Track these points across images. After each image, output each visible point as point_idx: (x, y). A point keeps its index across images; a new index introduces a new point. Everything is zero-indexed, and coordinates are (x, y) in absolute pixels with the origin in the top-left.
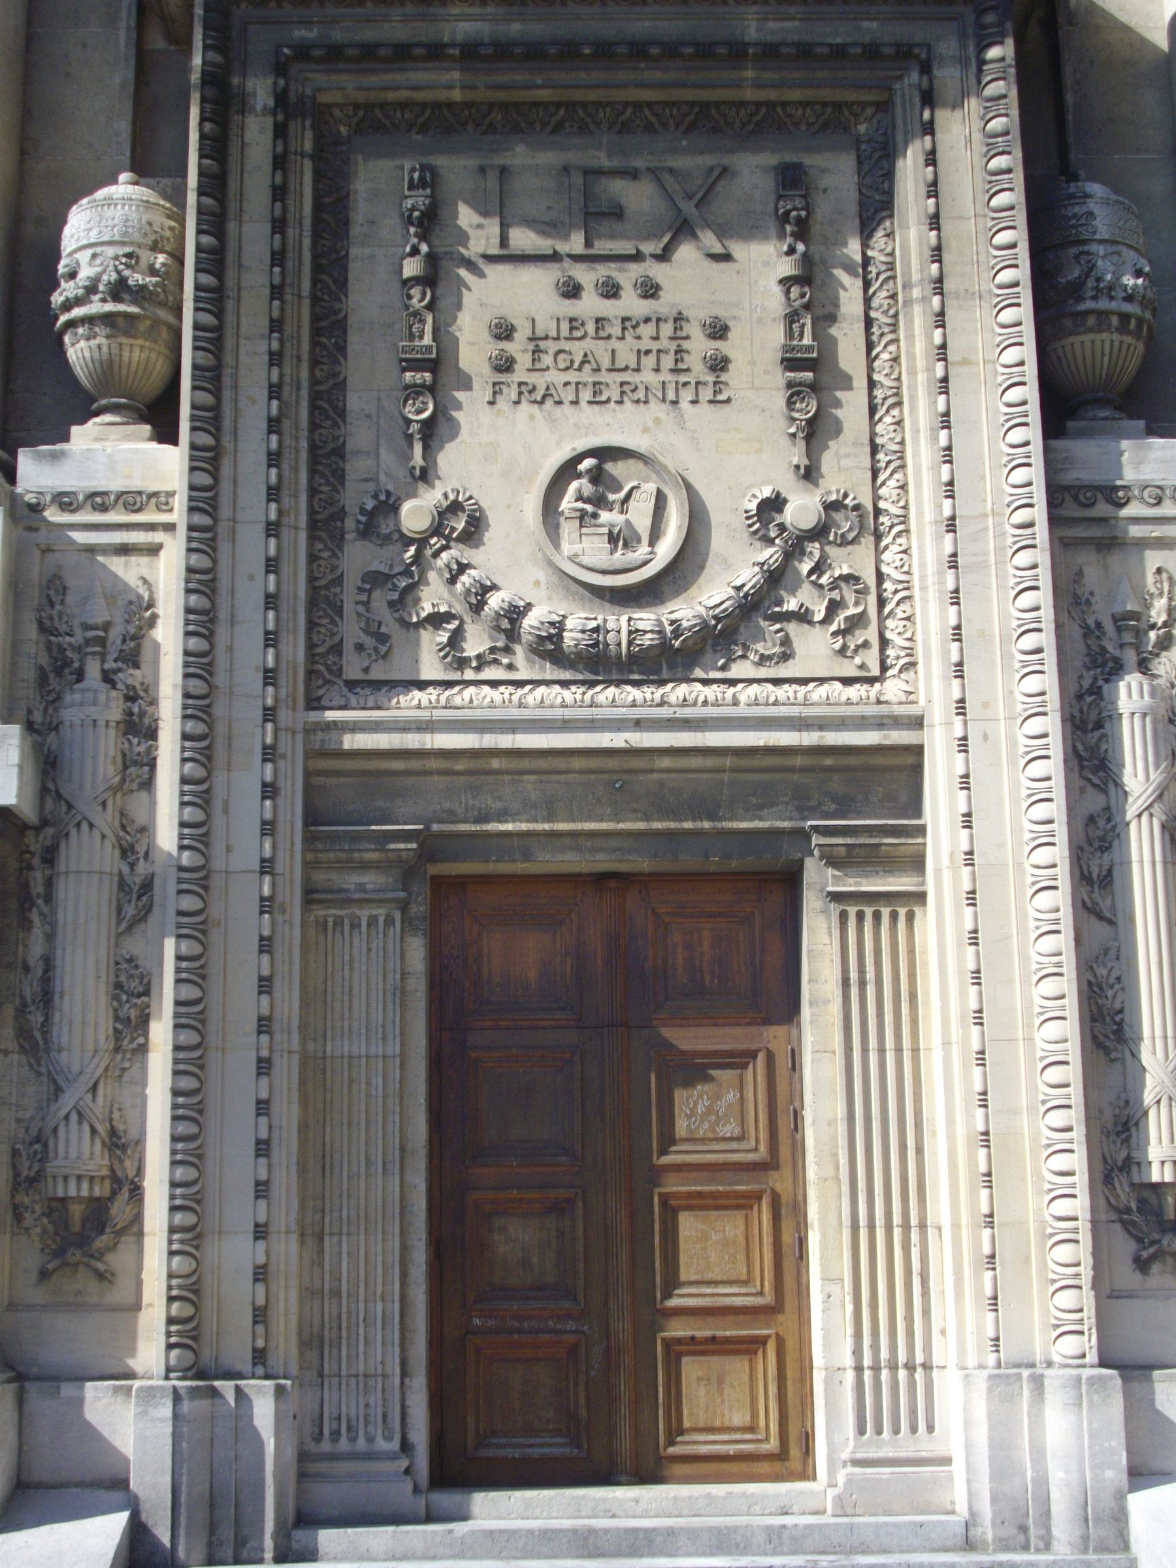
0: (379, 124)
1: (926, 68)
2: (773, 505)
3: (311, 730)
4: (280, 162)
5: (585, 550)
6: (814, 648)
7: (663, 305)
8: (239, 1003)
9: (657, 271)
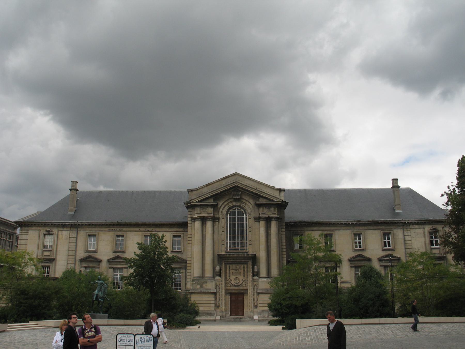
0: (227, 264)
6: (244, 285)
8: (223, 299)
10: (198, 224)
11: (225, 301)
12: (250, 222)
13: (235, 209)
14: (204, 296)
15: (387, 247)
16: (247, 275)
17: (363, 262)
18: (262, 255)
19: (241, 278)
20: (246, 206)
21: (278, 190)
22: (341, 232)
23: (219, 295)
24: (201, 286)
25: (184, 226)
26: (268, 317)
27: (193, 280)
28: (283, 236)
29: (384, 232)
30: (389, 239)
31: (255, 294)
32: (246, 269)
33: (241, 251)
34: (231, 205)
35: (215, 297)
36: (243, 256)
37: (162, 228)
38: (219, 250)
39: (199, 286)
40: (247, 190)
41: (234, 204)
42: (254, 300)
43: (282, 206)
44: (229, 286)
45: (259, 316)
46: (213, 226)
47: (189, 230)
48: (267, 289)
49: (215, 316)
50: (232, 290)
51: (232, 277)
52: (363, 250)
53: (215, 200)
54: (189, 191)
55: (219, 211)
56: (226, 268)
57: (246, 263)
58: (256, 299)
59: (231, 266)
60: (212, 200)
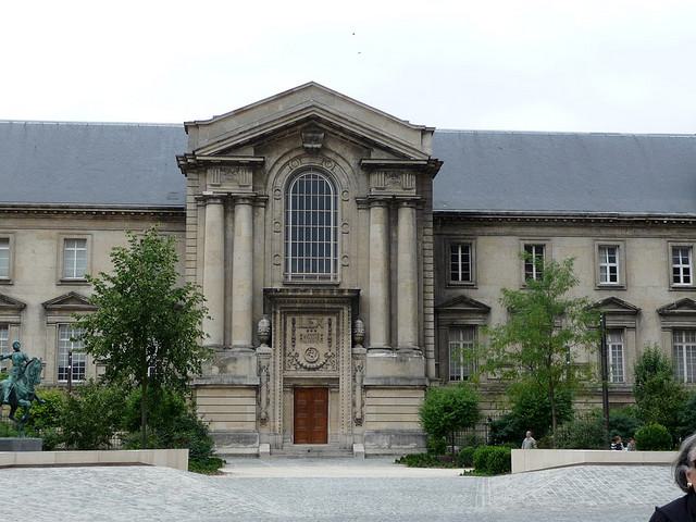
0: (289, 313)
5: (309, 358)
6: (330, 368)
10: (213, 212)
11: (281, 408)
12: (345, 209)
13: (308, 177)
14: (228, 393)
15: (682, 284)
17: (621, 318)
18: (375, 293)
19: (322, 348)
20: (337, 168)
21: (419, 130)
22: (568, 241)
24: (223, 368)
25: (174, 216)
28: (427, 246)
29: (675, 244)
30: (686, 261)
31: (358, 389)
32: (334, 327)
33: (321, 282)
34: (298, 165)
36: (328, 294)
37: (112, 220)
38: (268, 279)
39: (215, 370)
40: (341, 129)
41: (306, 162)
42: (354, 405)
43: (427, 171)
44: (293, 368)
46: (253, 216)
47: (188, 228)
48: (387, 378)
51: (301, 348)
52: (620, 288)
53: (257, 152)
54: (187, 127)
55: (267, 181)
56: (285, 323)
57: (335, 312)
58: (358, 404)
59: (297, 318)
60: (250, 151)
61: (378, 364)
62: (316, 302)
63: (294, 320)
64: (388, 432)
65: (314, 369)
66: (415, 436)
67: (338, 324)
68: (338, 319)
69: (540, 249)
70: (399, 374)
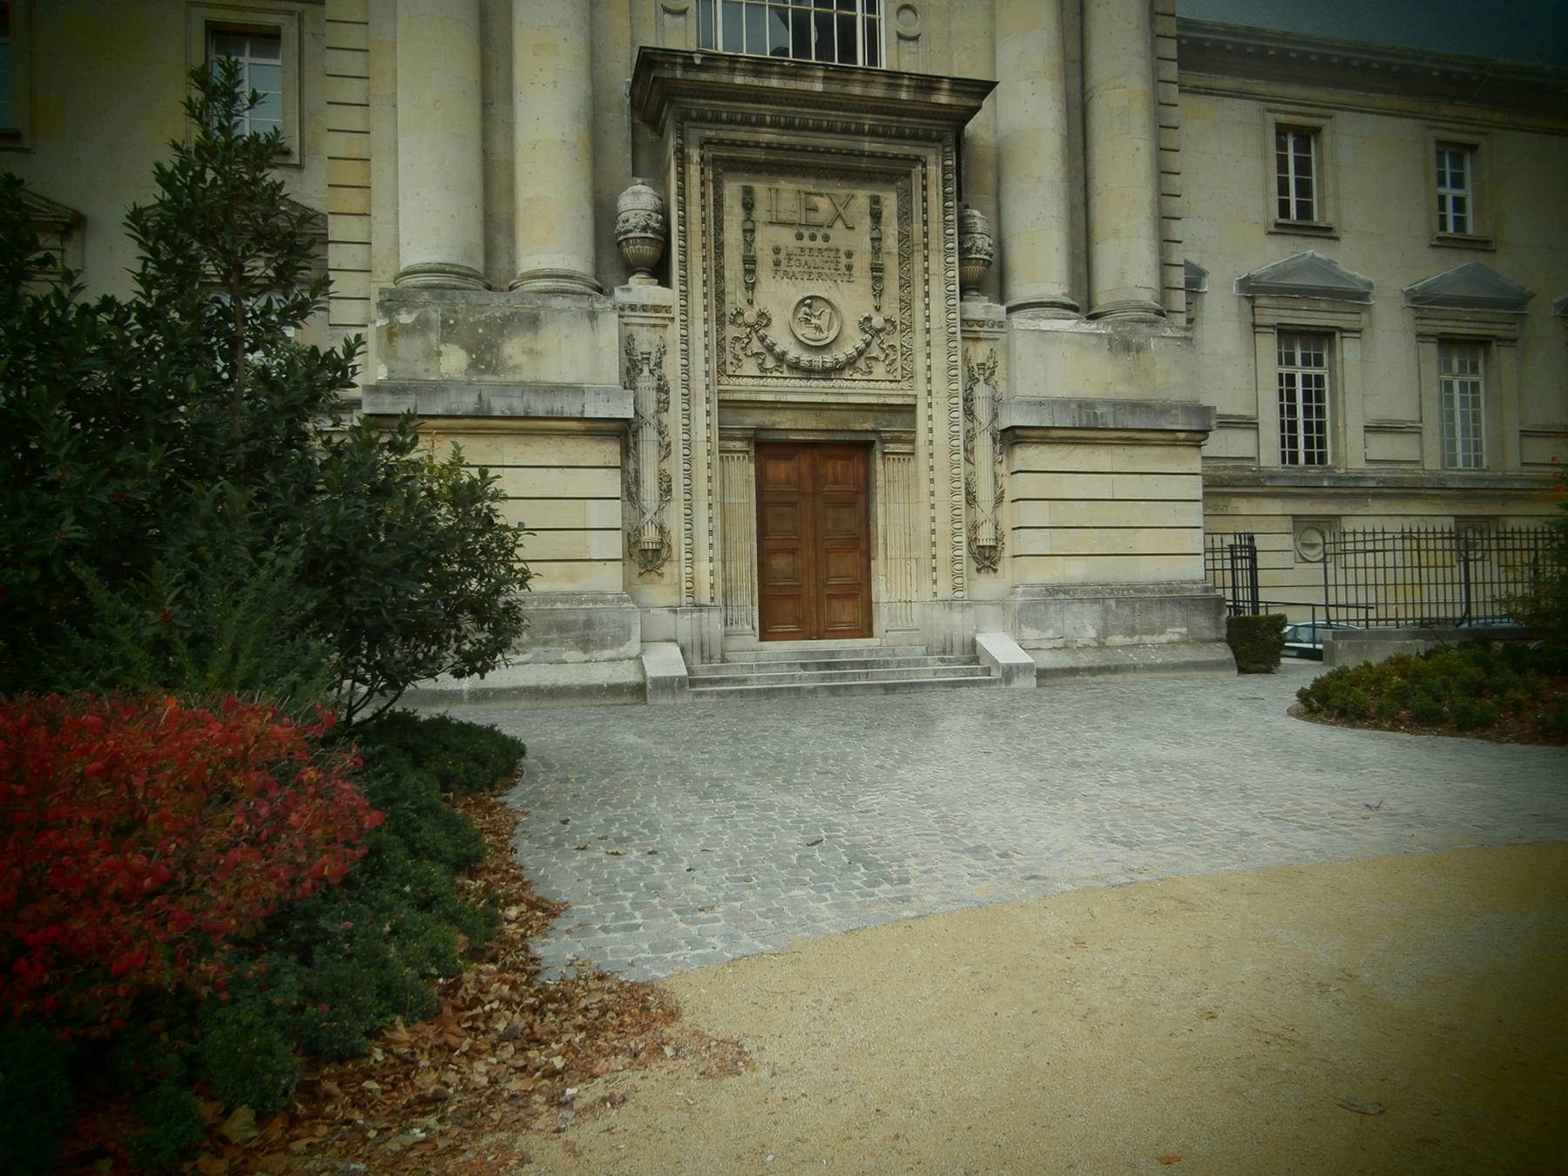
1: (924, 165)
2: (868, 319)
3: (720, 391)
4: (703, 184)
5: (806, 332)
6: (879, 370)
7: (831, 244)
8: (702, 486)
9: (830, 232)
11: (712, 514)
16: (906, 284)
23: (665, 449)
24: (484, 355)
26: (1101, 646)
27: (391, 302)
31: (984, 444)
32: (891, 228)
35: (622, 468)
36: (878, 91)
39: (454, 361)
42: (971, 499)
44: (750, 367)
45: (1031, 634)
48: (1084, 405)
49: (633, 647)
50: (773, 406)
57: (892, 173)
59: (760, 188)
61: (1053, 363)
62: (831, 130)
63: (748, 192)
64: (1097, 594)
65: (827, 373)
66: (1174, 601)
67: (905, 215)
68: (905, 197)
69: (1306, 136)
70: (1126, 391)
